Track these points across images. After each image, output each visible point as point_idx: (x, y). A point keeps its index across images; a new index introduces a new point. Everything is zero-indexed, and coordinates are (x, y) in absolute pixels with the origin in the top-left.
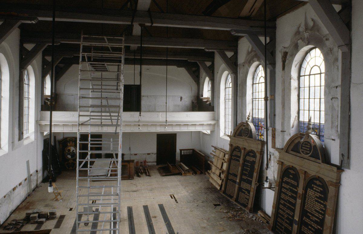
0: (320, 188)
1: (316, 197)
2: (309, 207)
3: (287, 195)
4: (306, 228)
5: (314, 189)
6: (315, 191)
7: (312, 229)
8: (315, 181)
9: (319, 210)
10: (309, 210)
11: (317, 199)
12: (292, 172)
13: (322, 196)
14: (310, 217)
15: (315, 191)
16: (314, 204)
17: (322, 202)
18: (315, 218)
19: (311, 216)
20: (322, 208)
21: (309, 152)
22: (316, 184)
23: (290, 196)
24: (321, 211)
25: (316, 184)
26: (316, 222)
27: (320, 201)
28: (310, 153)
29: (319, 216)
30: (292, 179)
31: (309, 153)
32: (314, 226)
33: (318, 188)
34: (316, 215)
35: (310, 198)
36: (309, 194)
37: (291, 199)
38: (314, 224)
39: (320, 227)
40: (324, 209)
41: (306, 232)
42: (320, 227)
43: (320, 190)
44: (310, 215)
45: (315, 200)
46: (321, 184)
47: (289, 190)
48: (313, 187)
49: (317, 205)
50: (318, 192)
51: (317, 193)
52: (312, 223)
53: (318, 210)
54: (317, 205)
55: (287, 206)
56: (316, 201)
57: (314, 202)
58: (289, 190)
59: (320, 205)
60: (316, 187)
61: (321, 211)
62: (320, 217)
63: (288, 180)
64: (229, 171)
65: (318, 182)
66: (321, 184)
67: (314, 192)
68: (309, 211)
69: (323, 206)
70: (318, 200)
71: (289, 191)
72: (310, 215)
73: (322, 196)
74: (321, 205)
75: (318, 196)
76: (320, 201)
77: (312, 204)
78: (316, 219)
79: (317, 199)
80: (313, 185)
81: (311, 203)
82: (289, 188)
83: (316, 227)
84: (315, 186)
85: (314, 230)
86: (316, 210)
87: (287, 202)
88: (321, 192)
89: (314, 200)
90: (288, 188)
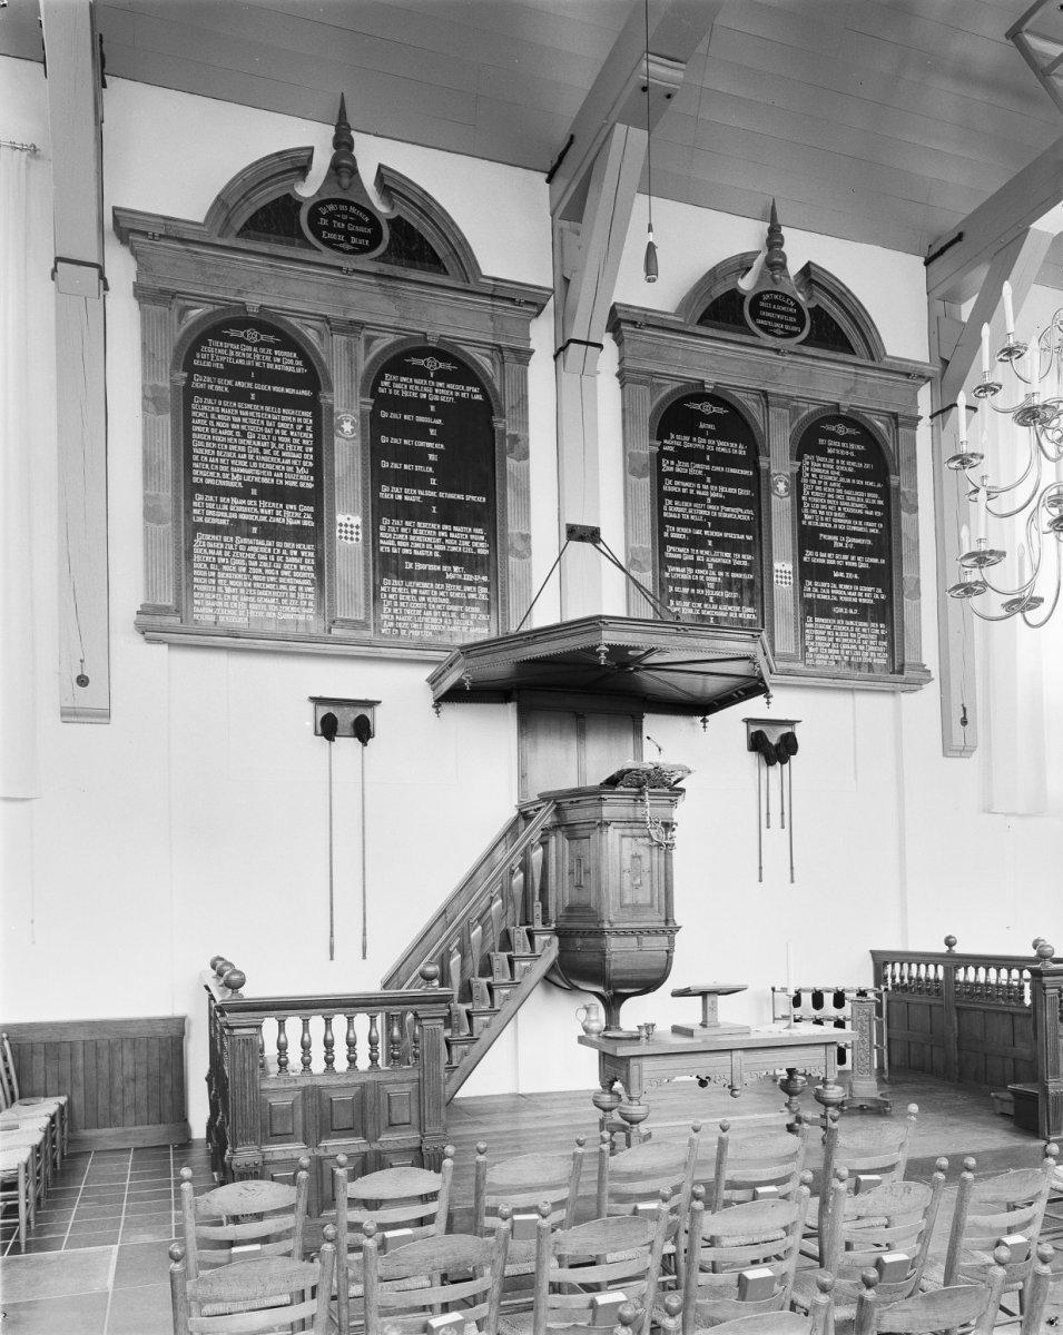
0: (852, 446)
1: (845, 474)
2: (821, 513)
3: (703, 500)
4: (824, 584)
5: (830, 451)
6: (835, 456)
7: (849, 575)
8: (828, 428)
9: (864, 510)
10: (824, 522)
11: (849, 481)
12: (707, 408)
13: (867, 466)
14: (832, 542)
15: (835, 456)
16: (839, 497)
17: (871, 484)
18: (854, 540)
19: (836, 538)
20: (874, 501)
21: (795, 329)
22: (834, 436)
23: (716, 501)
24: (871, 513)
25: (834, 436)
26: (859, 550)
27: (860, 482)
28: (802, 330)
29: (865, 530)
30: (713, 435)
31: (797, 334)
32: (854, 564)
33: (844, 445)
34: (854, 528)
35: (820, 482)
36: (810, 472)
37: (728, 509)
38: (853, 558)
39: (876, 561)
40: (881, 502)
41: (824, 597)
42: (876, 561)
43: (855, 451)
44: (830, 538)
45: (842, 484)
46: (854, 432)
47: (709, 480)
48: (826, 447)
49: (853, 499)
50: (847, 458)
51: (843, 462)
52: (846, 557)
53: (860, 512)
54: (853, 499)
55: (710, 543)
56: (845, 486)
57: (840, 491)
58: (709, 480)
59: (862, 494)
60: (835, 443)
61: (871, 513)
62: (872, 531)
63: (691, 441)
64: (317, 418)
65: (841, 430)
66: (854, 432)
67: (832, 460)
68: (822, 525)
69: (876, 496)
70: (854, 481)
71: (709, 485)
72: (830, 538)
73: (867, 466)
74: (869, 495)
75: (851, 470)
76: (860, 482)
77: (829, 502)
78: (859, 541)
79: (849, 481)
80: (821, 441)
81: (826, 498)
82: (704, 471)
83: (862, 566)
84: (831, 443)
85: (856, 577)
86: (849, 516)
87: (708, 529)
88: (859, 457)
89: (835, 488)
90: (700, 472)
